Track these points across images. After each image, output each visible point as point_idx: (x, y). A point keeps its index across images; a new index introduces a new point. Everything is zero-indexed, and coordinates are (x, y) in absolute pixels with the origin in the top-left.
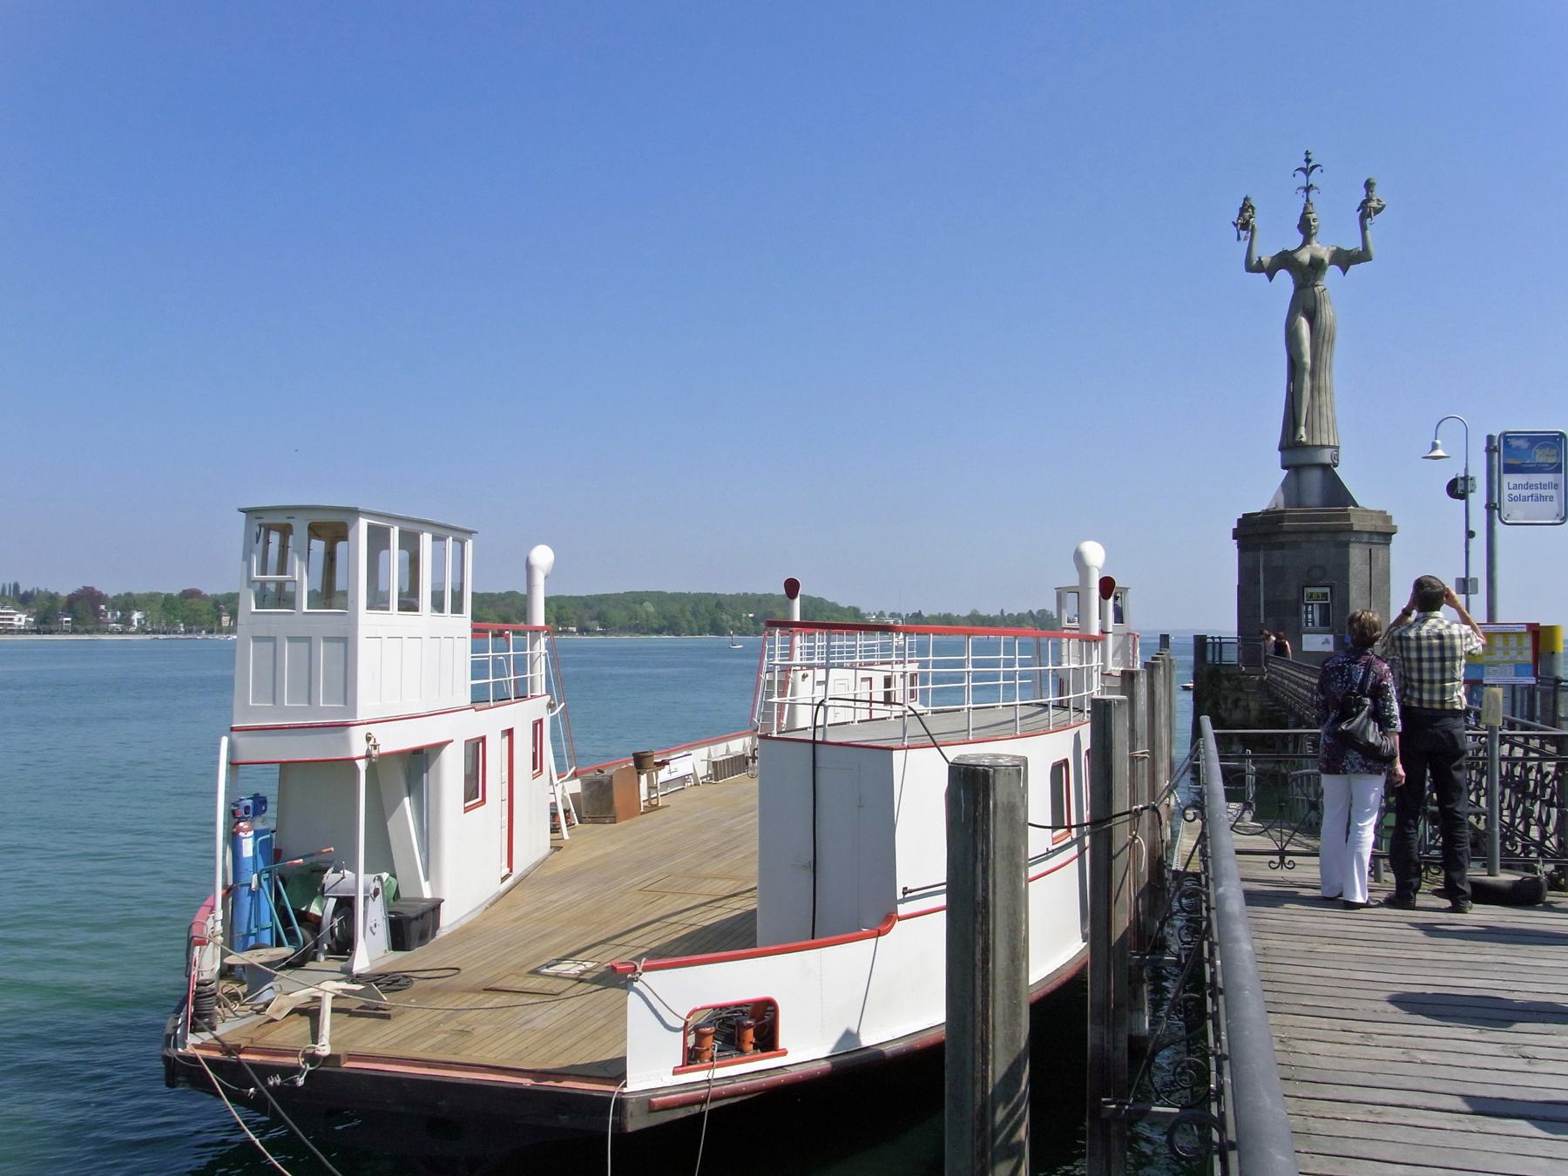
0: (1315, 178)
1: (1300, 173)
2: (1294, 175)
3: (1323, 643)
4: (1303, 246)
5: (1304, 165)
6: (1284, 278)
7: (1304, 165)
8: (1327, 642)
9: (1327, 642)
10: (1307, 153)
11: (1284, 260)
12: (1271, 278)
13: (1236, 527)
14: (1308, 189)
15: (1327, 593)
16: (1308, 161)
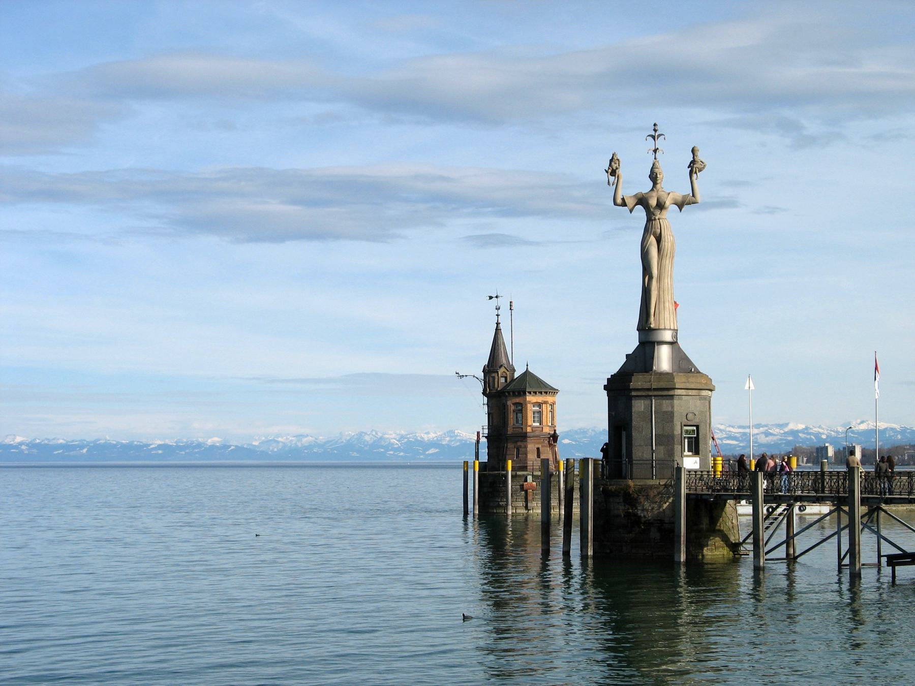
0: (660, 143)
1: (650, 139)
2: (646, 140)
3: (694, 463)
4: (652, 190)
5: (653, 133)
6: (640, 211)
7: (653, 133)
8: (696, 462)
9: (696, 462)
10: (655, 125)
11: (642, 201)
12: (631, 211)
13: (606, 384)
14: (655, 151)
15: (694, 430)
16: (655, 130)
